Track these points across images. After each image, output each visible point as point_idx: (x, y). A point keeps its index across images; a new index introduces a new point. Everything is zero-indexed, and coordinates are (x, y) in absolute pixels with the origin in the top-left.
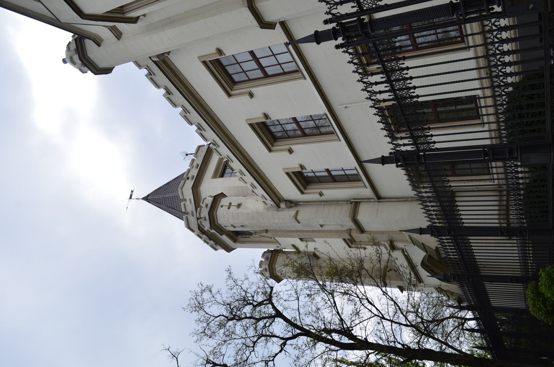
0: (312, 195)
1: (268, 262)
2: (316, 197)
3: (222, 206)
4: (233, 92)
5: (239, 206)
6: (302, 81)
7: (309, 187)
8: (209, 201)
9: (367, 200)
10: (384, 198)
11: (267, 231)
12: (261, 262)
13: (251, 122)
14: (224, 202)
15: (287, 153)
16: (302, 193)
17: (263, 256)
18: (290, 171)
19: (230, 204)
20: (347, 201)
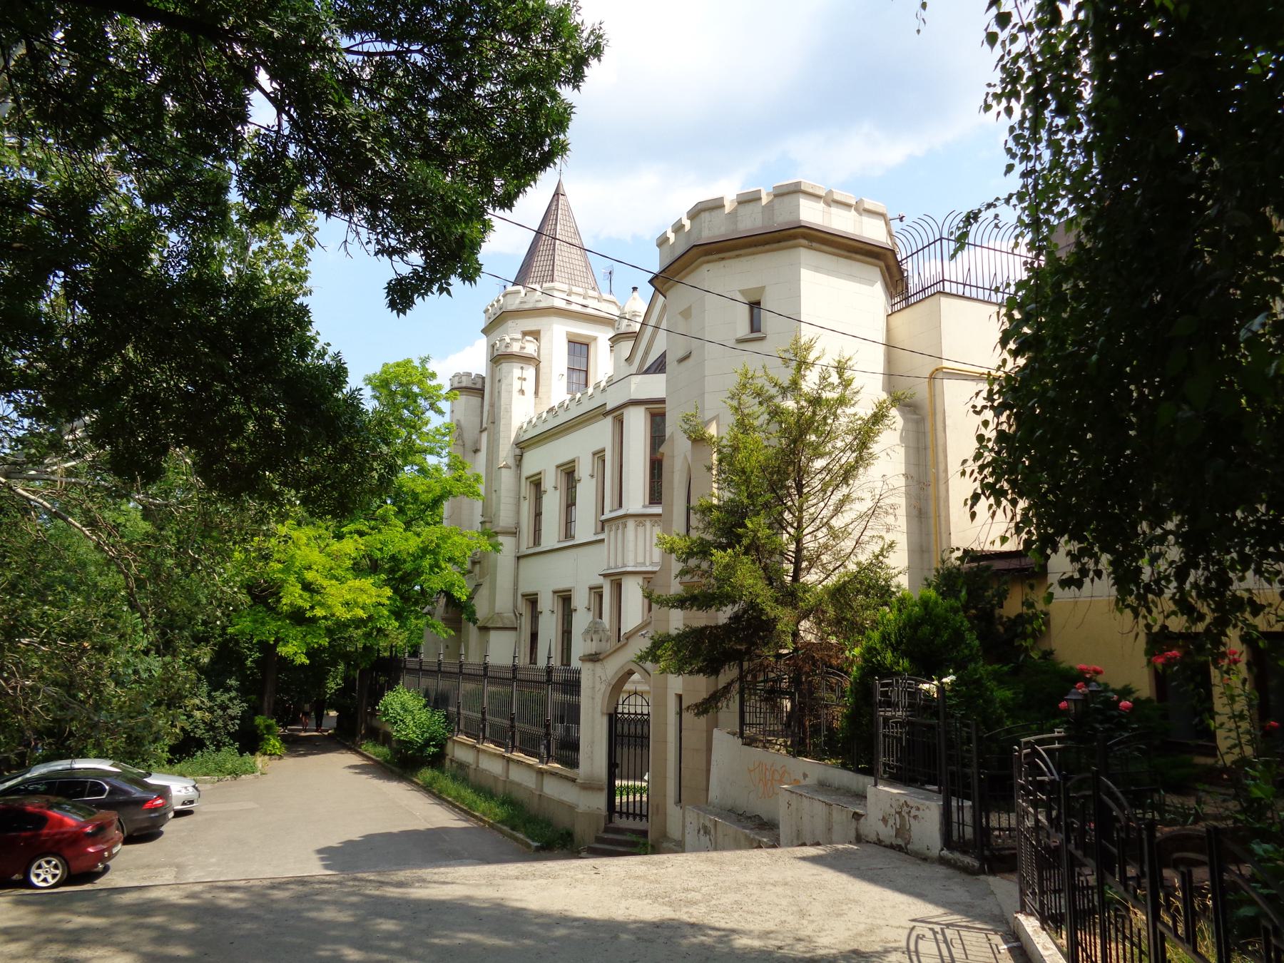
0: (527, 490)
1: (470, 385)
2: (523, 494)
3: (522, 368)
5: (522, 392)
6: (593, 531)
7: (533, 487)
8: (530, 348)
9: (518, 546)
11: (493, 423)
13: (576, 464)
14: (530, 372)
15: (554, 484)
16: (527, 479)
17: (478, 376)
18: (542, 475)
19: (525, 379)
20: (518, 523)
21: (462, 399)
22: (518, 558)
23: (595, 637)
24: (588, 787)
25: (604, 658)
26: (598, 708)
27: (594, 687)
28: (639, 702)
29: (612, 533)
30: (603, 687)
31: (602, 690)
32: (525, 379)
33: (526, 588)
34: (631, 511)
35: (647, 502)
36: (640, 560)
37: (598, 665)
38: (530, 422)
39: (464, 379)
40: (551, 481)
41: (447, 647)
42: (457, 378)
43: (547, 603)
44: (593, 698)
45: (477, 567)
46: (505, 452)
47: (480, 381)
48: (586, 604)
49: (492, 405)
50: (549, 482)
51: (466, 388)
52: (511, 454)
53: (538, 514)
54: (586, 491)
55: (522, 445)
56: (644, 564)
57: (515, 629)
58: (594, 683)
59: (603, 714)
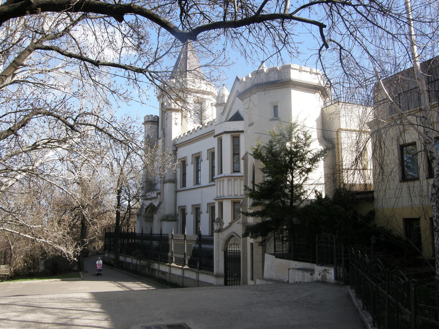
1: (152, 120)
4: (209, 151)
5: (176, 124)
6: (208, 181)
10: (176, 194)
12: (153, 115)
19: (177, 119)
20: (176, 178)
21: (149, 126)
22: (176, 192)
23: (218, 224)
24: (217, 276)
25: (223, 231)
26: (221, 249)
27: (219, 242)
28: (235, 247)
29: (218, 184)
30: (222, 242)
31: (222, 242)
32: (177, 119)
33: (179, 204)
34: (226, 175)
35: (232, 172)
36: (230, 194)
37: (220, 233)
38: (180, 136)
39: (150, 117)
40: (189, 161)
41: (146, 228)
42: (147, 117)
43: (189, 210)
44: (219, 246)
45: (159, 196)
46: (170, 150)
47: (156, 118)
48: (206, 210)
49: (163, 130)
50: (189, 161)
51: (151, 121)
52: (171, 149)
53: (184, 175)
54: (205, 165)
55: (177, 146)
56: (231, 195)
57: (176, 221)
58: (219, 240)
59: (222, 250)
